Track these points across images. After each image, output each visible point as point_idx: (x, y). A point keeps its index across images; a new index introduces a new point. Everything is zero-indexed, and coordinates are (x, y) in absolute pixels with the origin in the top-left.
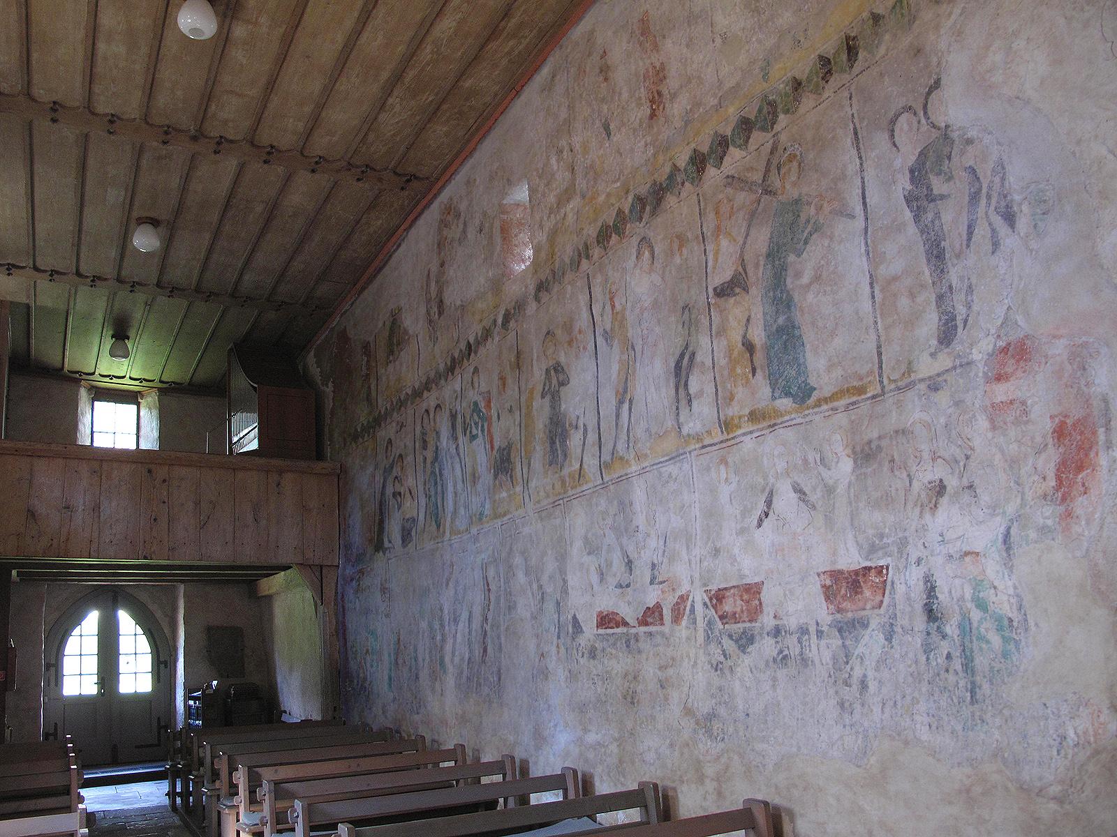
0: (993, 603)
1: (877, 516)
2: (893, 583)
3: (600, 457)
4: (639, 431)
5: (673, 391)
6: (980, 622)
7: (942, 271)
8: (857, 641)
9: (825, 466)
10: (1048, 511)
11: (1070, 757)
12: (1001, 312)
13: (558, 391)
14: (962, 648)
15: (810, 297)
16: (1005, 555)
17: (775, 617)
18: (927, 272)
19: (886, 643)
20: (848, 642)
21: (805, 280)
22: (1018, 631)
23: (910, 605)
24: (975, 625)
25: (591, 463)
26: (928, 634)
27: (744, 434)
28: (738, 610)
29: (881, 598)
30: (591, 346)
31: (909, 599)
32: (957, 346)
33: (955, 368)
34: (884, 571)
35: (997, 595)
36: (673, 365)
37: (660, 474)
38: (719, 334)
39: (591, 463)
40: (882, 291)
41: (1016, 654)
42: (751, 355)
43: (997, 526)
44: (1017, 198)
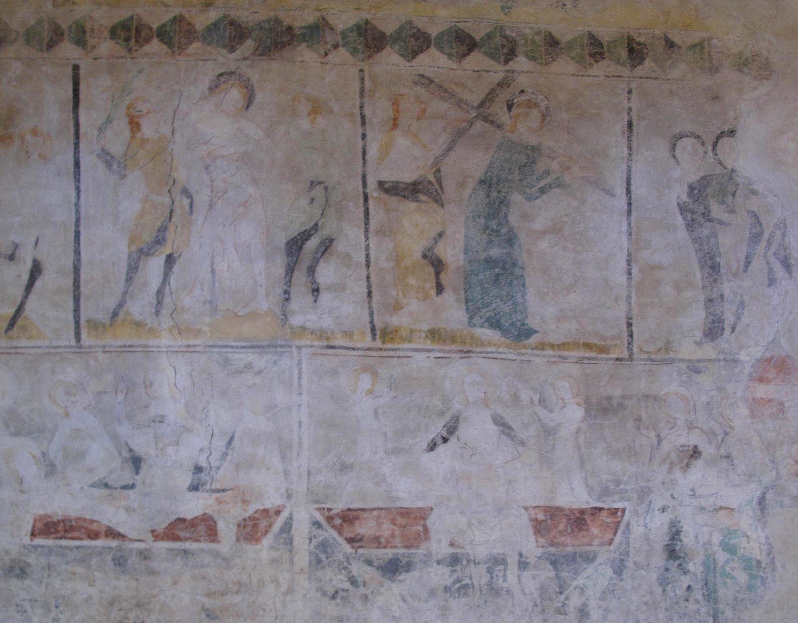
2: (628, 524)
16: (758, 513)
19: (615, 576)
34: (620, 514)
35: (748, 543)
37: (226, 362)
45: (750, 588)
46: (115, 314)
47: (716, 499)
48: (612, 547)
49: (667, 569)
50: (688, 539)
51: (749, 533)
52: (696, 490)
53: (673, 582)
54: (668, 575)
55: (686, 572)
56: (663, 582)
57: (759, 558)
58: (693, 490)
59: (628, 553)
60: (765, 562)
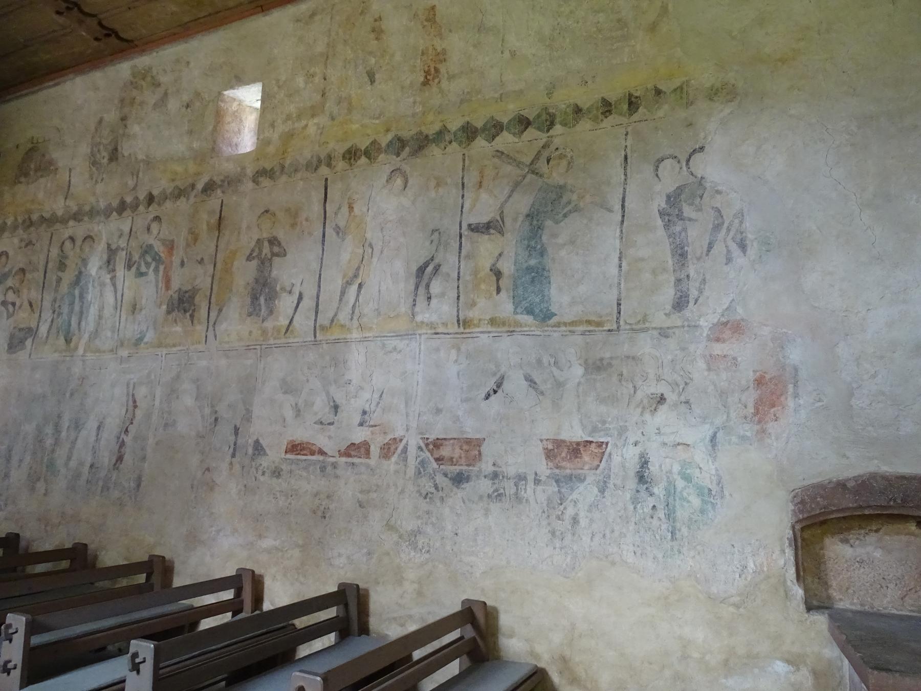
1: (603, 409)
3: (316, 320)
4: (368, 309)
5: (413, 288)
7: (683, 265)
8: (572, 490)
9: (558, 368)
12: (726, 302)
13: (270, 260)
15: (563, 253)
16: (710, 448)
17: (494, 465)
18: (670, 262)
20: (563, 490)
21: (560, 241)
25: (303, 322)
26: (638, 491)
27: (482, 332)
28: (456, 456)
30: (318, 233)
32: (687, 313)
33: (683, 327)
36: (414, 268)
37: (384, 345)
38: (468, 257)
39: (303, 322)
40: (629, 264)
42: (498, 280)
43: (706, 431)
44: (749, 236)
45: (702, 511)
46: (332, 321)
51: (701, 466)
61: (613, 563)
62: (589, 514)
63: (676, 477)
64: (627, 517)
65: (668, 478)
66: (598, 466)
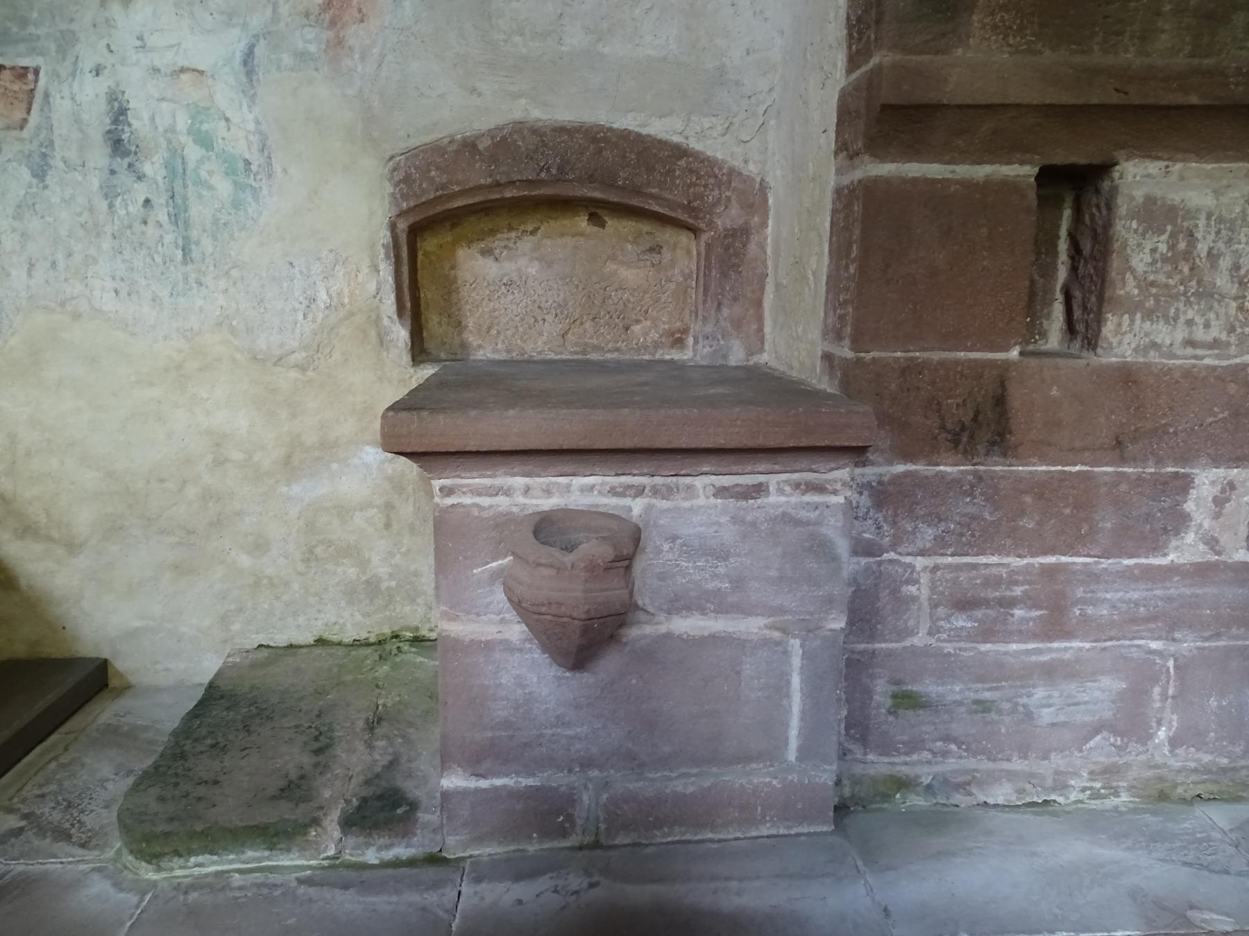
0: (223, 139)
6: (201, 161)
10: (310, 33)
11: (319, 320)
14: (170, 194)
16: (244, 79)
22: (259, 177)
23: (80, 130)
24: (191, 165)
29: (23, 115)
31: (78, 121)
41: (253, 204)
47: (177, 53)
48: (26, 133)
49: (113, 172)
50: (139, 122)
52: (145, 37)
53: (124, 193)
54: (115, 182)
55: (140, 177)
56: (110, 193)
57: (247, 156)
58: (140, 38)
59: (52, 143)
60: (257, 163)
61: (77, 316)
62: (16, 224)
63: (183, 139)
64: (96, 225)
65: (169, 142)
66: (25, 121)
